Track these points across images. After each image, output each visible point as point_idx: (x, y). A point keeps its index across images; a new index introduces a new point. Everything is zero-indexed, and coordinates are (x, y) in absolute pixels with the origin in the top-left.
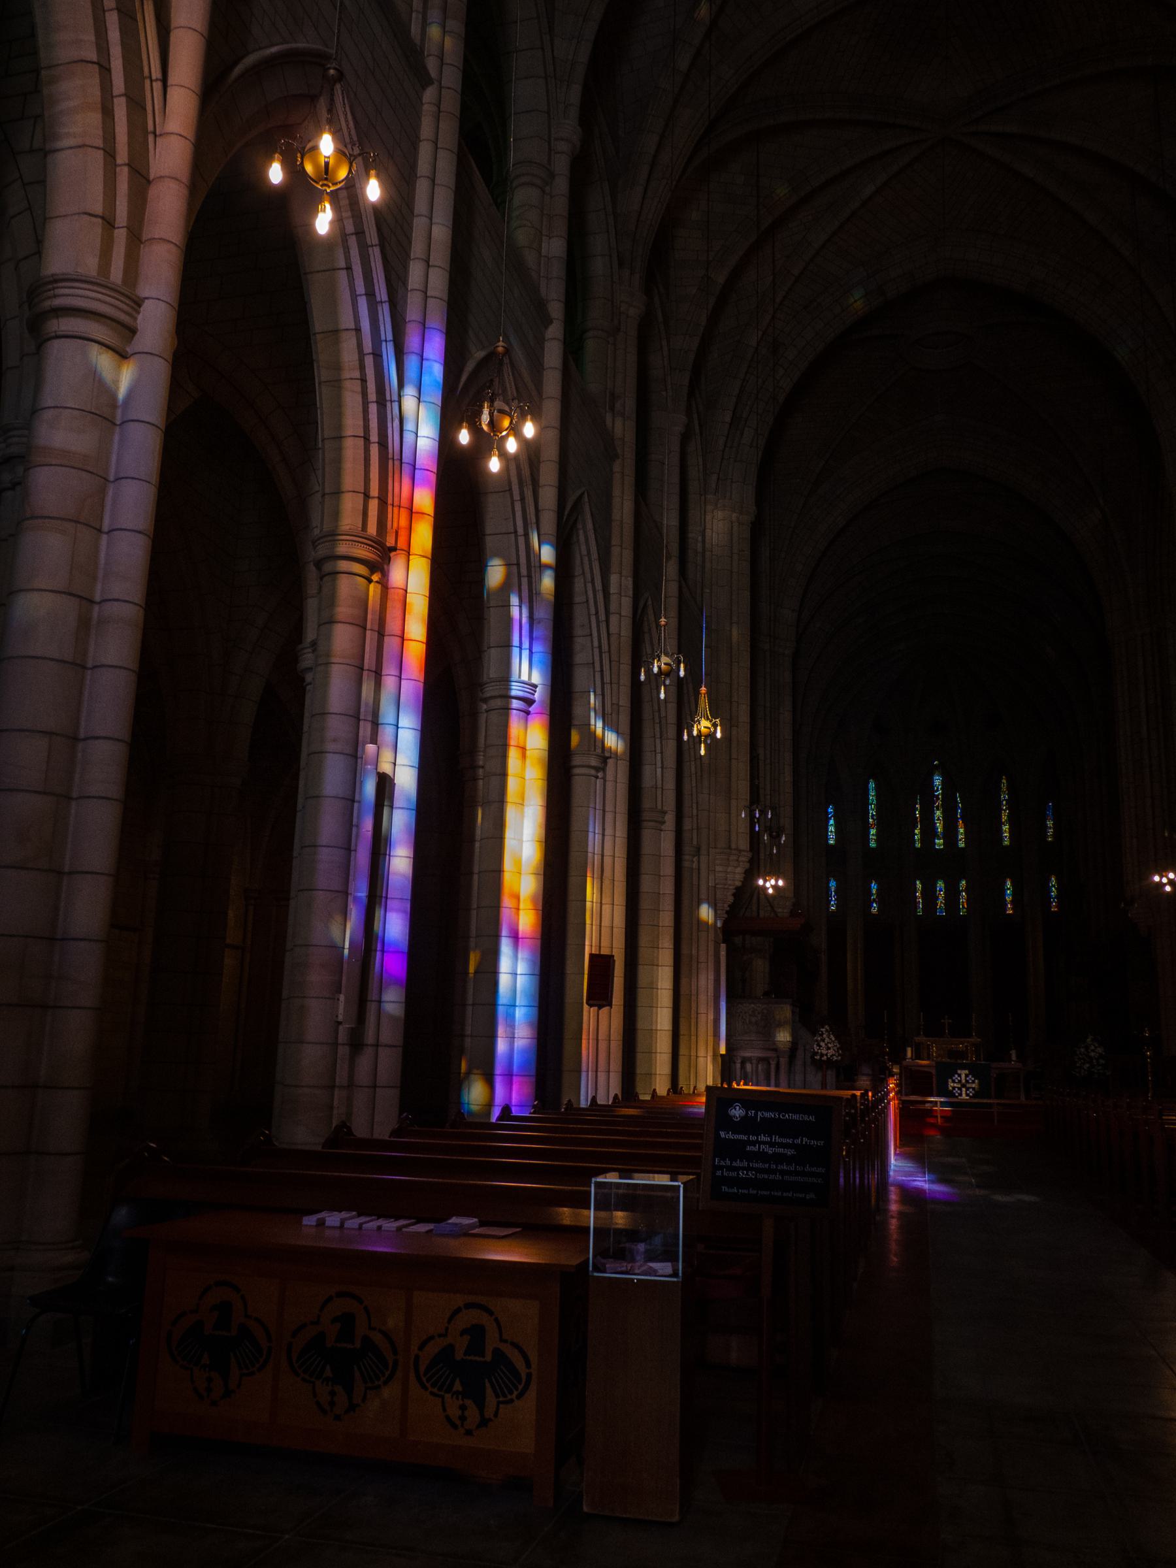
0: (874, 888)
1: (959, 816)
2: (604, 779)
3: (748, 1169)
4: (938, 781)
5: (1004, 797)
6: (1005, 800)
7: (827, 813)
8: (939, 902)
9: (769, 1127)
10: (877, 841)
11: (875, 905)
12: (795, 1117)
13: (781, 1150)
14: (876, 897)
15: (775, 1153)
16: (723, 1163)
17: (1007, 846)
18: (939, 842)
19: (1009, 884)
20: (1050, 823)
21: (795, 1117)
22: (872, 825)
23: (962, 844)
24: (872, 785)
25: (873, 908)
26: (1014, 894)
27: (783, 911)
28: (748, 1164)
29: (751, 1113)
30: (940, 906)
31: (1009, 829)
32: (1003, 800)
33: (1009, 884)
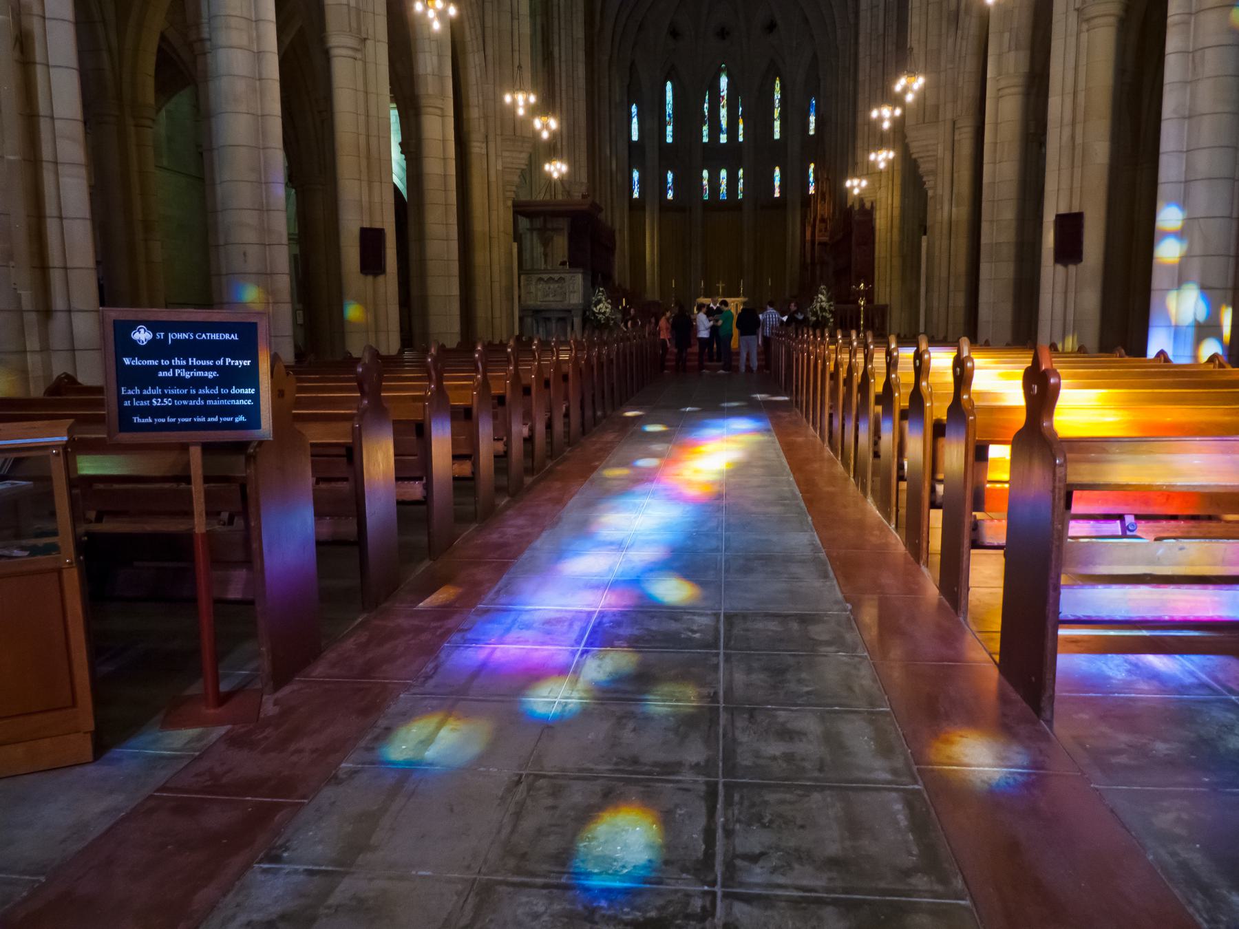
0: (670, 176)
1: (740, 114)
2: (365, 63)
3: (163, 396)
4: (724, 81)
5: (777, 96)
7: (630, 113)
8: (722, 188)
9: (184, 349)
10: (674, 136)
12: (215, 336)
13: (200, 374)
15: (193, 377)
16: (130, 392)
17: (777, 140)
18: (723, 139)
20: (812, 119)
21: (215, 336)
23: (741, 139)
24: (669, 86)
25: (668, 195)
26: (781, 180)
27: (578, 194)
28: (163, 392)
29: (160, 335)
31: (781, 124)
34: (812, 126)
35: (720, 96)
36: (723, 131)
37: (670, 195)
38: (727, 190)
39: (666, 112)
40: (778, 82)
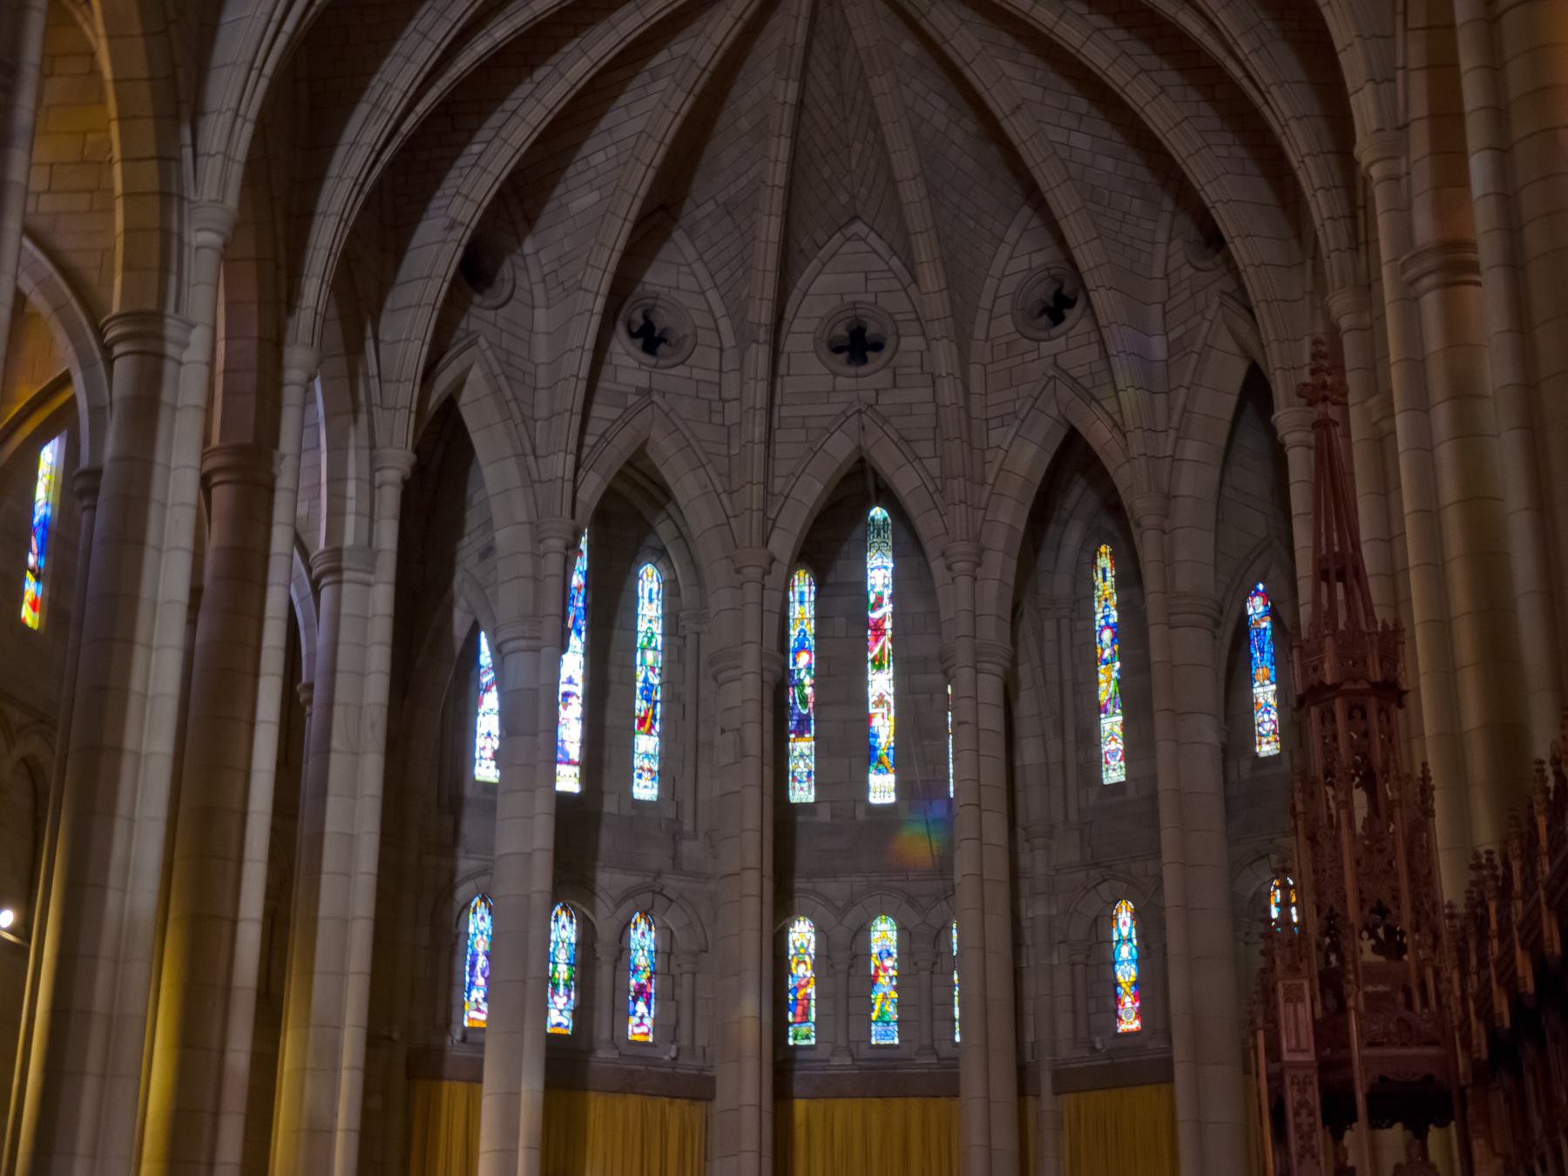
0: (643, 941)
4: (879, 572)
5: (1106, 609)
6: (1108, 626)
8: (877, 997)
10: (666, 776)
11: (641, 1007)
14: (649, 979)
17: (1117, 786)
18: (882, 788)
19: (1124, 921)
20: (1264, 692)
22: (642, 722)
24: (649, 580)
25: (634, 1020)
30: (882, 1013)
31: (1125, 726)
32: (1103, 628)
33: (1124, 921)
34: (1267, 722)
35: (865, 623)
36: (880, 762)
37: (641, 1024)
38: (900, 1006)
39: (634, 680)
40: (1104, 562)
